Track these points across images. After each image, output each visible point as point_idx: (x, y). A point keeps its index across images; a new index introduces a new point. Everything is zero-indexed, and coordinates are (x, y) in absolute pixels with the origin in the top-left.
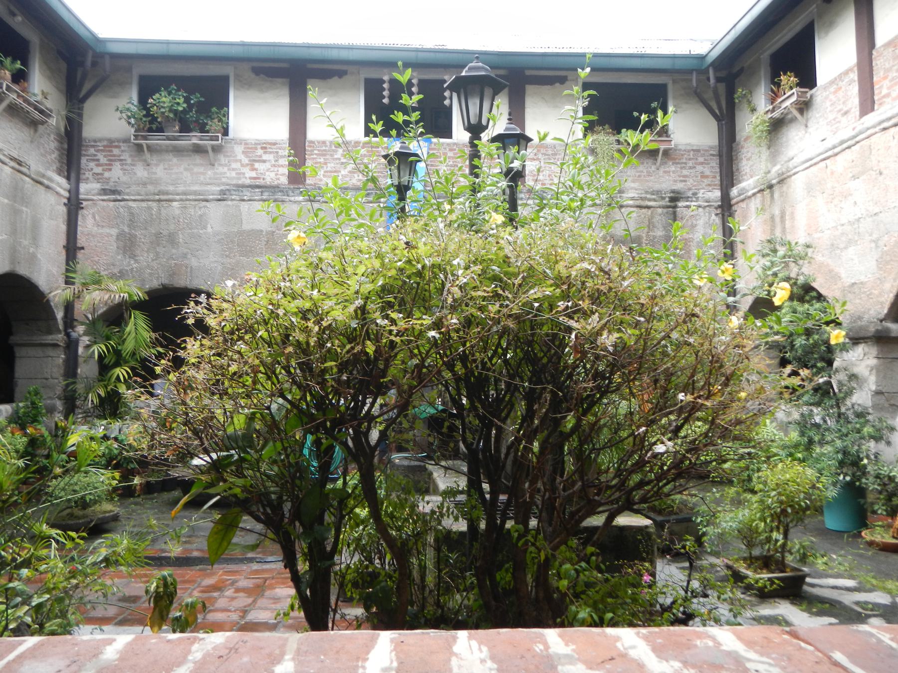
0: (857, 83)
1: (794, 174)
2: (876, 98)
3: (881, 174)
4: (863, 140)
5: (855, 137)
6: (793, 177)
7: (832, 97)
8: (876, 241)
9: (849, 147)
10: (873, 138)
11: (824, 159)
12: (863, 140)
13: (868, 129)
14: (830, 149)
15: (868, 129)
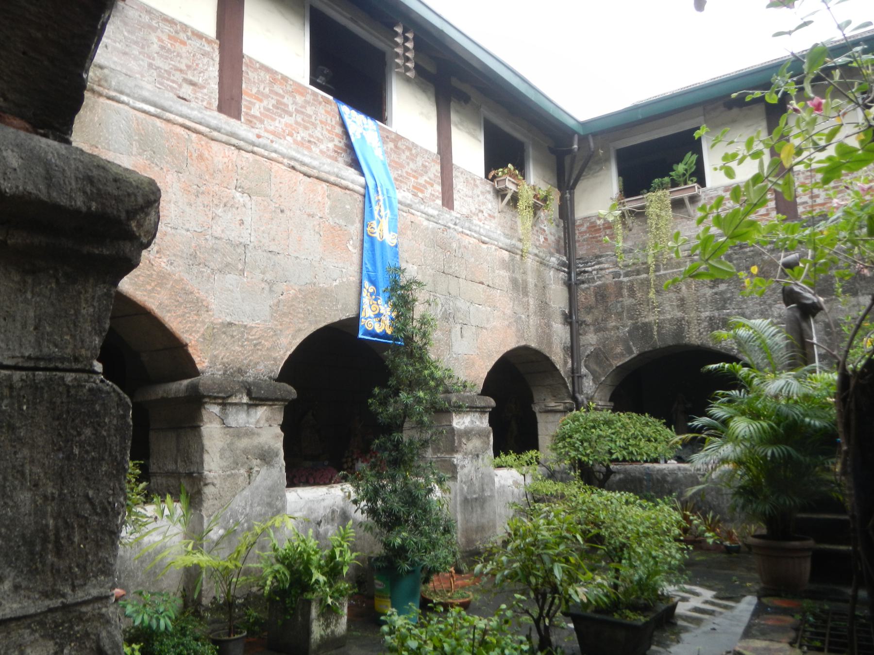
0: (217, 67)
1: (109, 98)
2: (243, 109)
3: (282, 211)
4: (263, 156)
5: (254, 145)
6: (102, 100)
7: (165, 38)
8: (271, 284)
9: (239, 148)
10: (275, 166)
11: (188, 128)
12: (263, 156)
13: (275, 152)
14: (208, 126)
15: (275, 152)
